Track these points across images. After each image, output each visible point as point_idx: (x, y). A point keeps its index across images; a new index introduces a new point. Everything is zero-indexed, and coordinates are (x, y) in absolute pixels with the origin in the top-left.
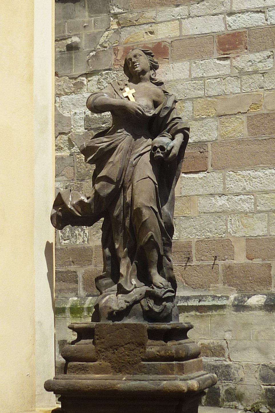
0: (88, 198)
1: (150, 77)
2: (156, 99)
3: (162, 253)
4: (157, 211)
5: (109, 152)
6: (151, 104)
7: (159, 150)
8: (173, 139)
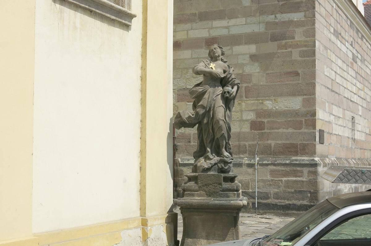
0: (193, 115)
1: (221, 58)
2: (225, 69)
3: (227, 141)
4: (225, 121)
5: (203, 93)
6: (222, 71)
7: (227, 93)
8: (232, 88)
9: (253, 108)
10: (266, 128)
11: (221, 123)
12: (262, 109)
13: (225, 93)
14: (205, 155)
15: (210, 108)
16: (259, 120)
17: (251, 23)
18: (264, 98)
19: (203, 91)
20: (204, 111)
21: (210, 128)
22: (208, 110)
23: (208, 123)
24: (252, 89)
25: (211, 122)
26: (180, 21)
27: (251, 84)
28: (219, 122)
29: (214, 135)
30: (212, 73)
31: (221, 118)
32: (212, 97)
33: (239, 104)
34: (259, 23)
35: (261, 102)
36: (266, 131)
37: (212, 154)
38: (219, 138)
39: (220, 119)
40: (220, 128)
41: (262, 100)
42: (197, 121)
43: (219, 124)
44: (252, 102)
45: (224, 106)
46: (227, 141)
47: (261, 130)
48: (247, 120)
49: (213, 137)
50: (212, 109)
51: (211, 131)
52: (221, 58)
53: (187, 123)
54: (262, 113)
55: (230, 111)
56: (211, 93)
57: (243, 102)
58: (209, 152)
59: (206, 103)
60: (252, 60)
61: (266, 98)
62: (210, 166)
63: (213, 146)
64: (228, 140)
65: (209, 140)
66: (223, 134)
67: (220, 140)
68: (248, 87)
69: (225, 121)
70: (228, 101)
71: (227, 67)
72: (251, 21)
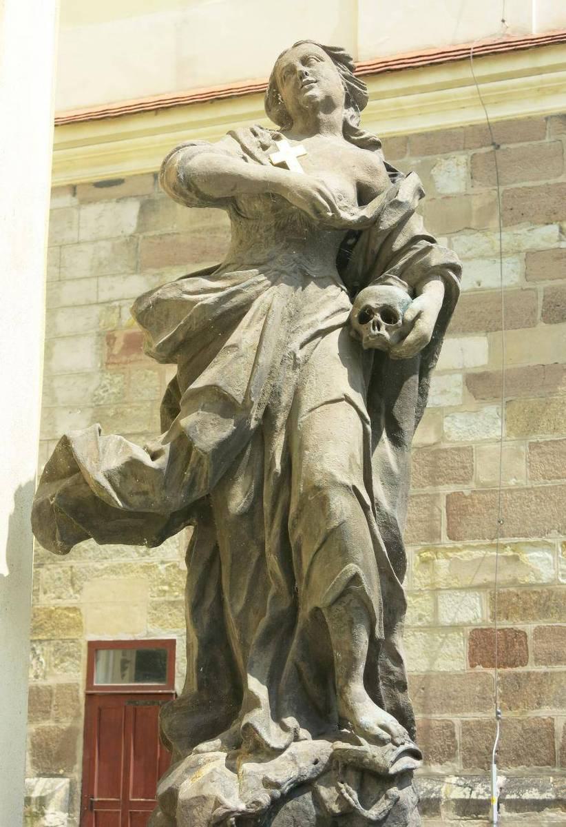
0: (154, 456)
1: (345, 123)
2: (365, 178)
3: (379, 633)
4: (369, 502)
5: (225, 320)
6: (352, 193)
7: (378, 317)
8: (414, 294)
9: (479, 580)
10: (531, 656)
11: (343, 506)
12: (514, 582)
13: (365, 316)
14: (236, 727)
15: (268, 415)
16: (505, 624)
17: (469, 254)
18: (523, 539)
19: (228, 305)
20: (229, 427)
21: (272, 542)
22: (253, 424)
23: (252, 512)
24: (473, 506)
25: (274, 506)
26: (204, 252)
27: (473, 485)
28: (324, 502)
29: (294, 593)
30: (287, 189)
31: (342, 478)
32: (283, 345)
33: (425, 562)
34: (501, 254)
35: (511, 553)
36: (531, 667)
37: (277, 716)
38: (330, 607)
39: (335, 483)
40: (334, 542)
41: (515, 547)
42: (178, 499)
43: (329, 517)
44: (478, 554)
45: (359, 399)
46: (379, 633)
47: (513, 665)
48: (455, 627)
49: (285, 604)
50: (281, 420)
51: (273, 563)
52: (345, 123)
53: (117, 510)
54: (514, 599)
55: (397, 441)
56: (275, 320)
57: (440, 555)
58: (256, 703)
59: (244, 375)
60: (475, 395)
61: (531, 540)
62: (265, 798)
63: (288, 664)
64: (390, 628)
65: (263, 623)
66: (356, 578)
67: (331, 627)
68: (460, 495)
69: (369, 502)
70: (387, 373)
71: (385, 173)
72: (470, 250)
